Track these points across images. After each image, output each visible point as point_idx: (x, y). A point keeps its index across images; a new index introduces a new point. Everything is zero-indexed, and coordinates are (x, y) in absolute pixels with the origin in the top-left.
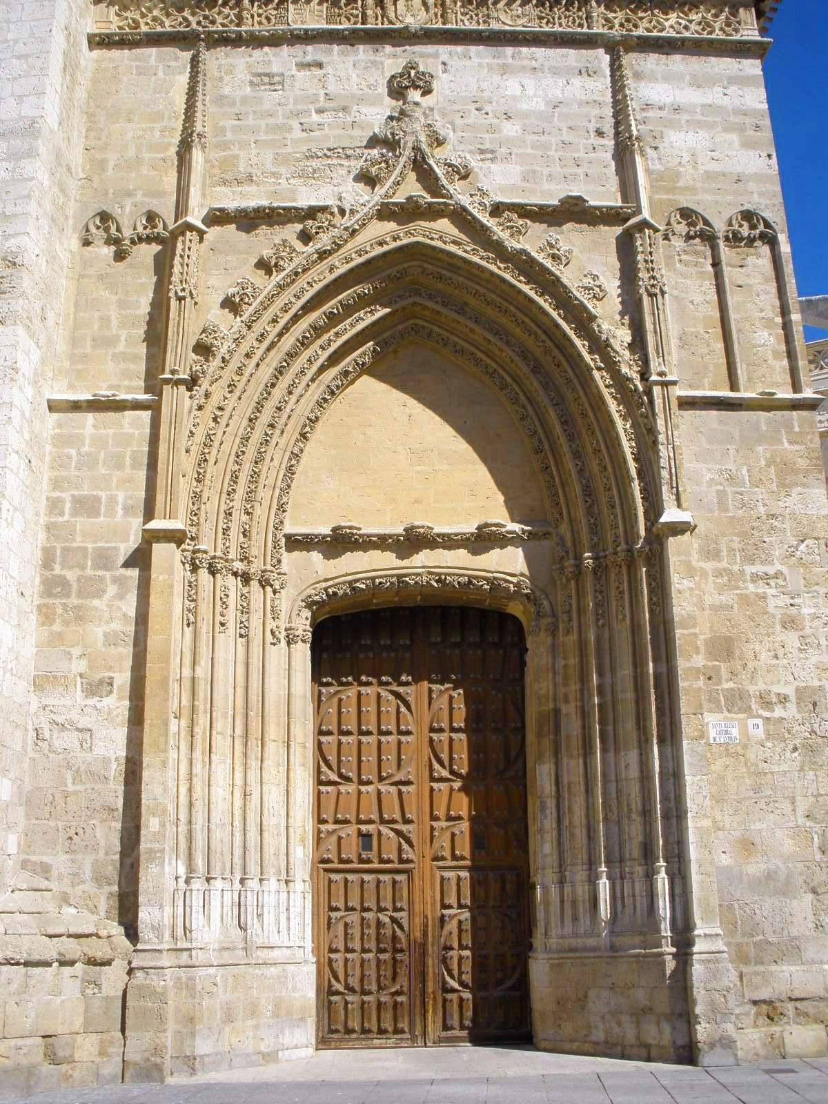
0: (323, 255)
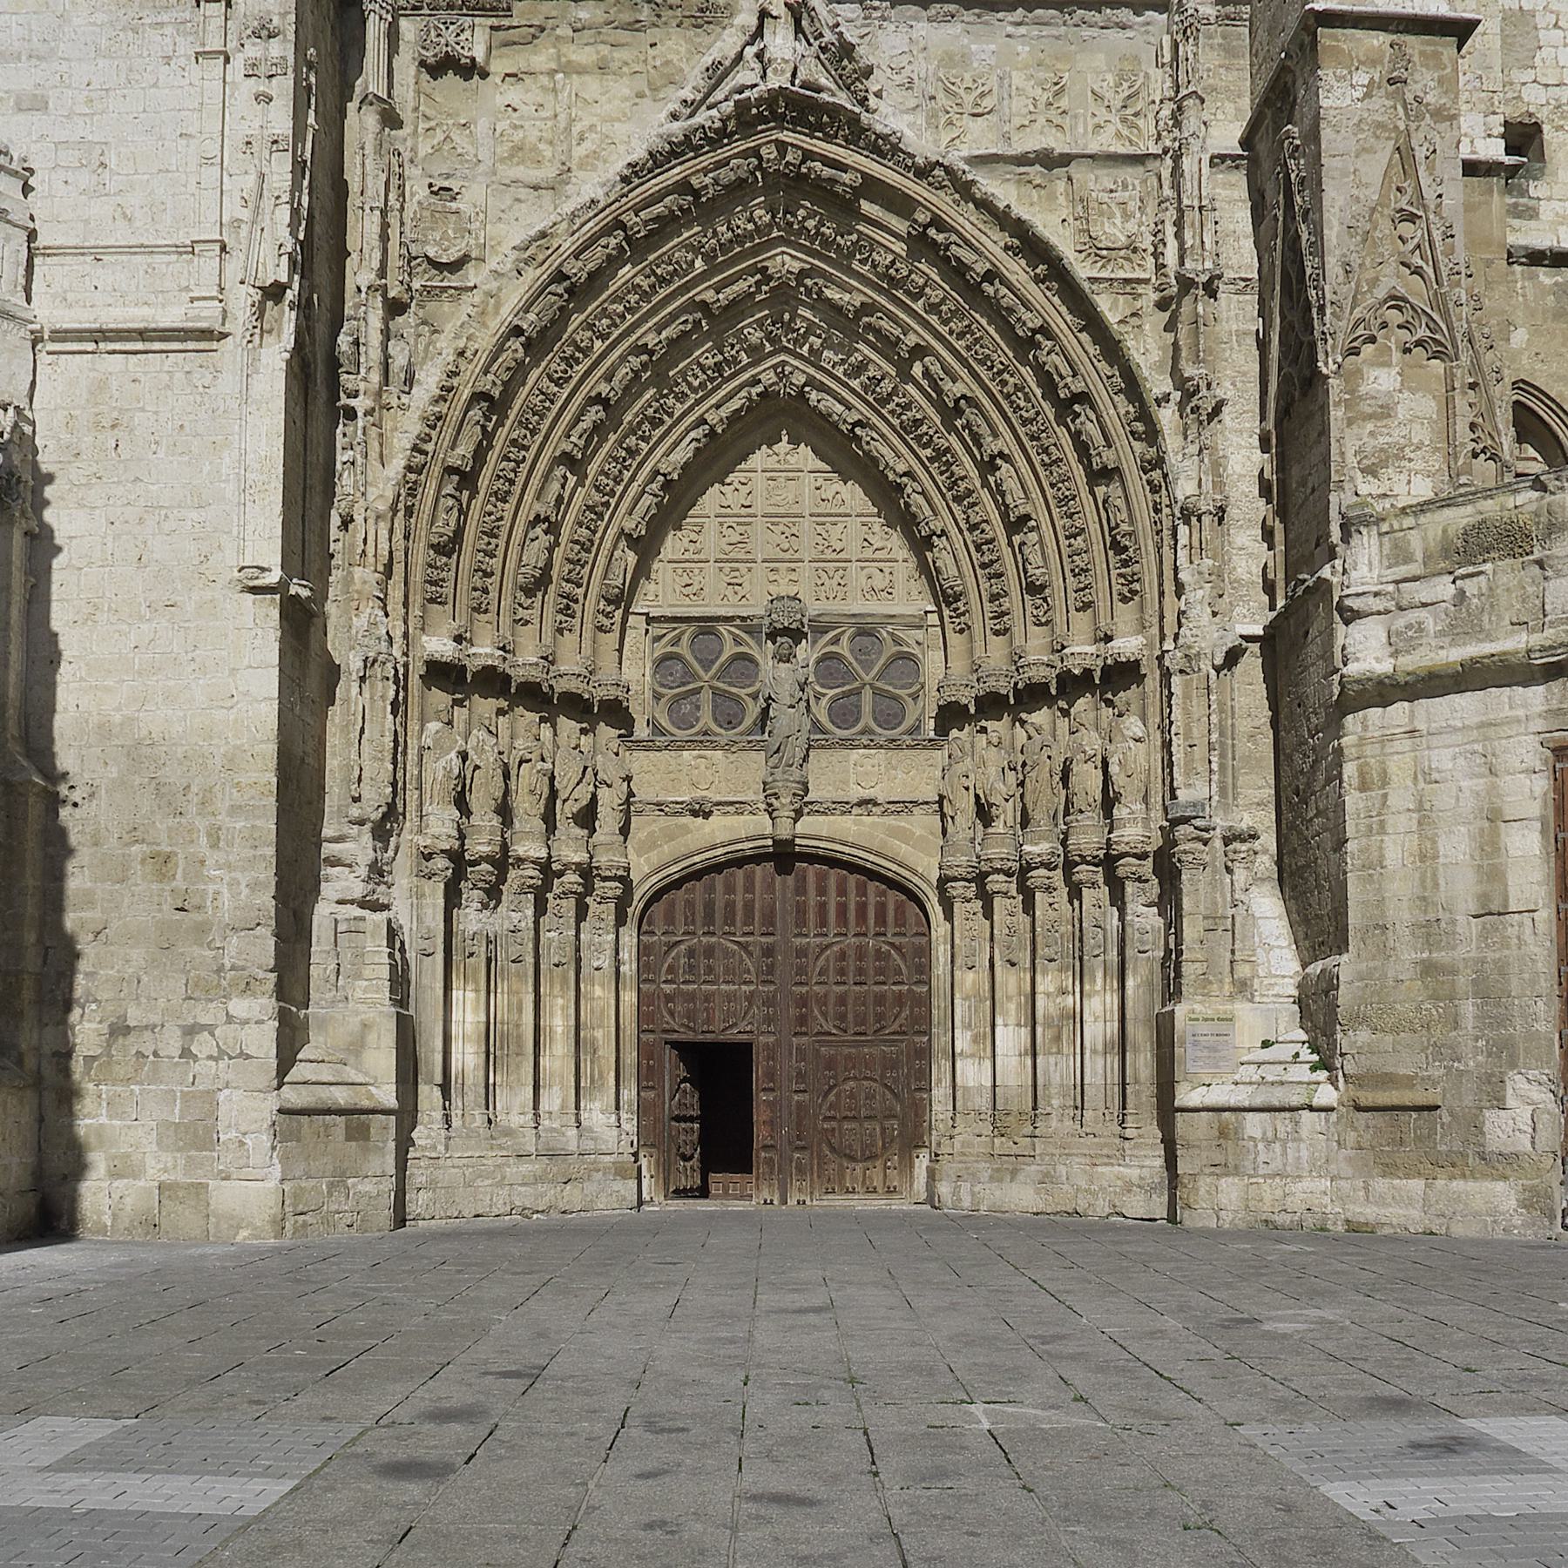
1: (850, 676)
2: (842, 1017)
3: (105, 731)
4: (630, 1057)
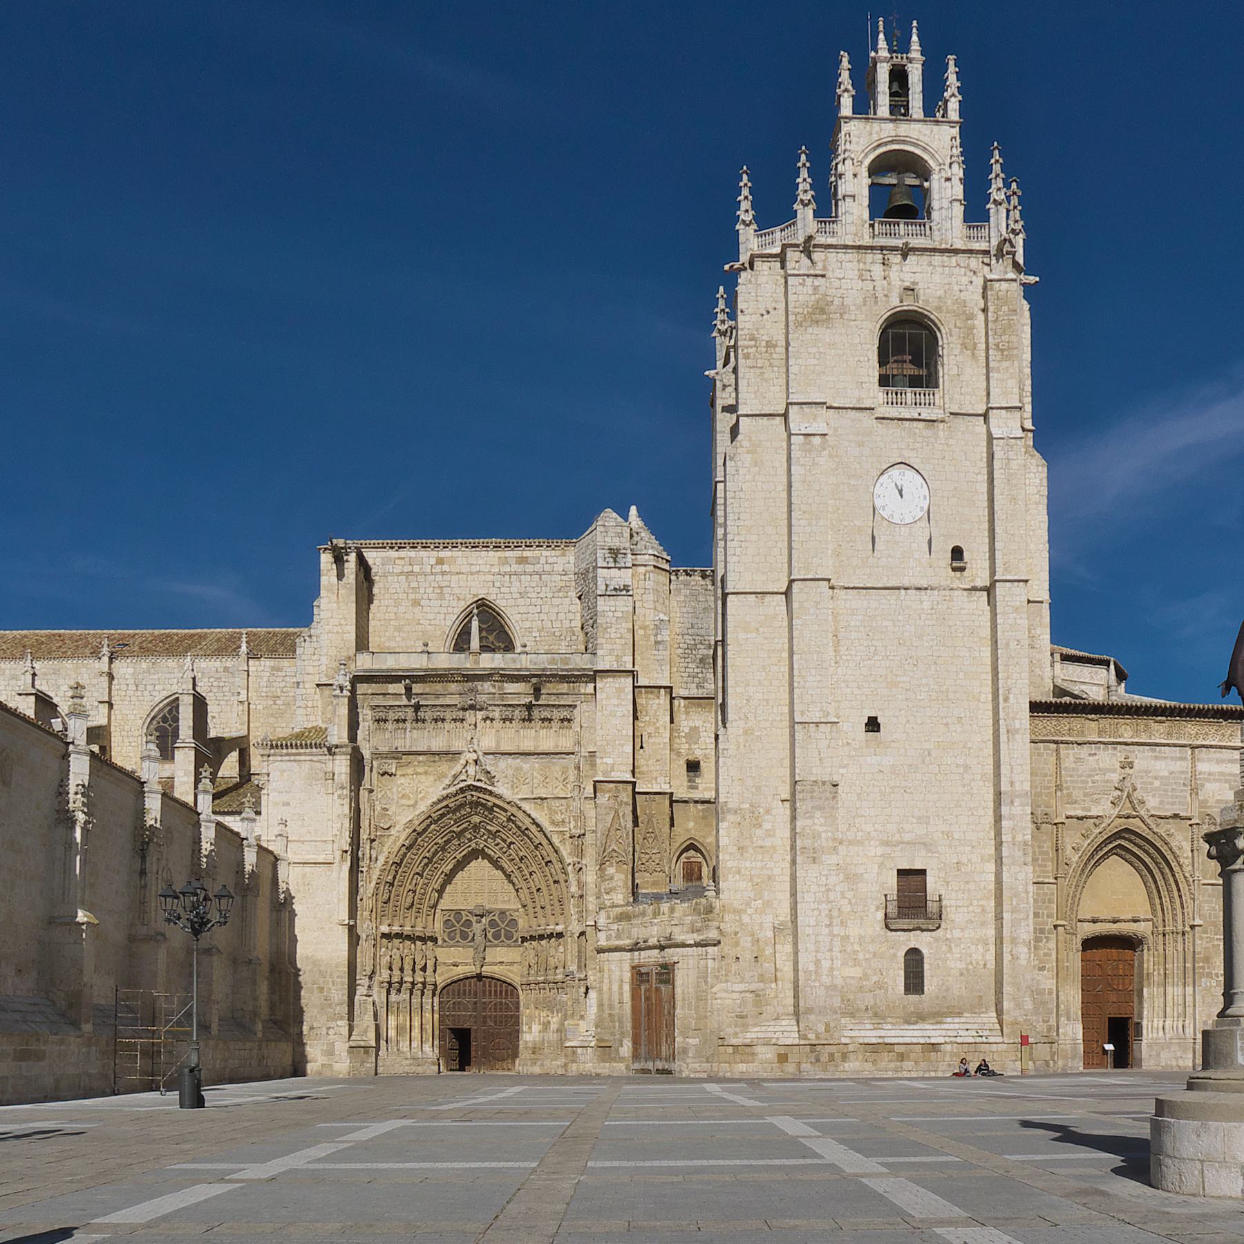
0: (1100, 833)
1: (498, 926)
2: (496, 1021)
3: (307, 958)
4: (437, 1032)
